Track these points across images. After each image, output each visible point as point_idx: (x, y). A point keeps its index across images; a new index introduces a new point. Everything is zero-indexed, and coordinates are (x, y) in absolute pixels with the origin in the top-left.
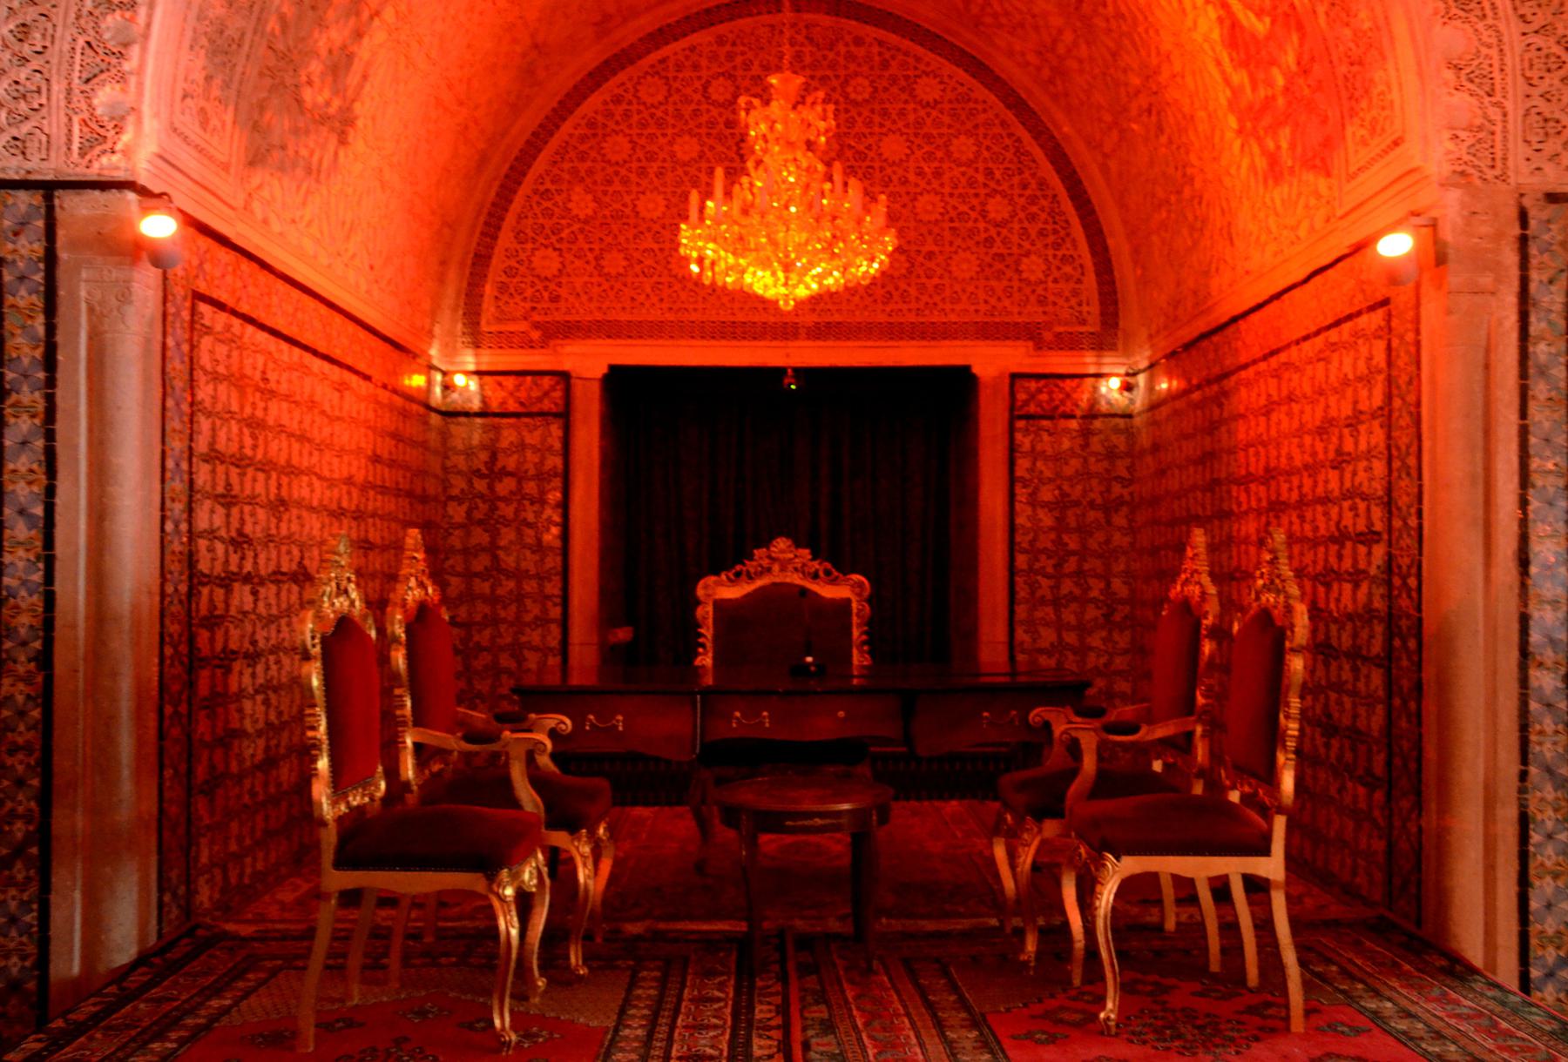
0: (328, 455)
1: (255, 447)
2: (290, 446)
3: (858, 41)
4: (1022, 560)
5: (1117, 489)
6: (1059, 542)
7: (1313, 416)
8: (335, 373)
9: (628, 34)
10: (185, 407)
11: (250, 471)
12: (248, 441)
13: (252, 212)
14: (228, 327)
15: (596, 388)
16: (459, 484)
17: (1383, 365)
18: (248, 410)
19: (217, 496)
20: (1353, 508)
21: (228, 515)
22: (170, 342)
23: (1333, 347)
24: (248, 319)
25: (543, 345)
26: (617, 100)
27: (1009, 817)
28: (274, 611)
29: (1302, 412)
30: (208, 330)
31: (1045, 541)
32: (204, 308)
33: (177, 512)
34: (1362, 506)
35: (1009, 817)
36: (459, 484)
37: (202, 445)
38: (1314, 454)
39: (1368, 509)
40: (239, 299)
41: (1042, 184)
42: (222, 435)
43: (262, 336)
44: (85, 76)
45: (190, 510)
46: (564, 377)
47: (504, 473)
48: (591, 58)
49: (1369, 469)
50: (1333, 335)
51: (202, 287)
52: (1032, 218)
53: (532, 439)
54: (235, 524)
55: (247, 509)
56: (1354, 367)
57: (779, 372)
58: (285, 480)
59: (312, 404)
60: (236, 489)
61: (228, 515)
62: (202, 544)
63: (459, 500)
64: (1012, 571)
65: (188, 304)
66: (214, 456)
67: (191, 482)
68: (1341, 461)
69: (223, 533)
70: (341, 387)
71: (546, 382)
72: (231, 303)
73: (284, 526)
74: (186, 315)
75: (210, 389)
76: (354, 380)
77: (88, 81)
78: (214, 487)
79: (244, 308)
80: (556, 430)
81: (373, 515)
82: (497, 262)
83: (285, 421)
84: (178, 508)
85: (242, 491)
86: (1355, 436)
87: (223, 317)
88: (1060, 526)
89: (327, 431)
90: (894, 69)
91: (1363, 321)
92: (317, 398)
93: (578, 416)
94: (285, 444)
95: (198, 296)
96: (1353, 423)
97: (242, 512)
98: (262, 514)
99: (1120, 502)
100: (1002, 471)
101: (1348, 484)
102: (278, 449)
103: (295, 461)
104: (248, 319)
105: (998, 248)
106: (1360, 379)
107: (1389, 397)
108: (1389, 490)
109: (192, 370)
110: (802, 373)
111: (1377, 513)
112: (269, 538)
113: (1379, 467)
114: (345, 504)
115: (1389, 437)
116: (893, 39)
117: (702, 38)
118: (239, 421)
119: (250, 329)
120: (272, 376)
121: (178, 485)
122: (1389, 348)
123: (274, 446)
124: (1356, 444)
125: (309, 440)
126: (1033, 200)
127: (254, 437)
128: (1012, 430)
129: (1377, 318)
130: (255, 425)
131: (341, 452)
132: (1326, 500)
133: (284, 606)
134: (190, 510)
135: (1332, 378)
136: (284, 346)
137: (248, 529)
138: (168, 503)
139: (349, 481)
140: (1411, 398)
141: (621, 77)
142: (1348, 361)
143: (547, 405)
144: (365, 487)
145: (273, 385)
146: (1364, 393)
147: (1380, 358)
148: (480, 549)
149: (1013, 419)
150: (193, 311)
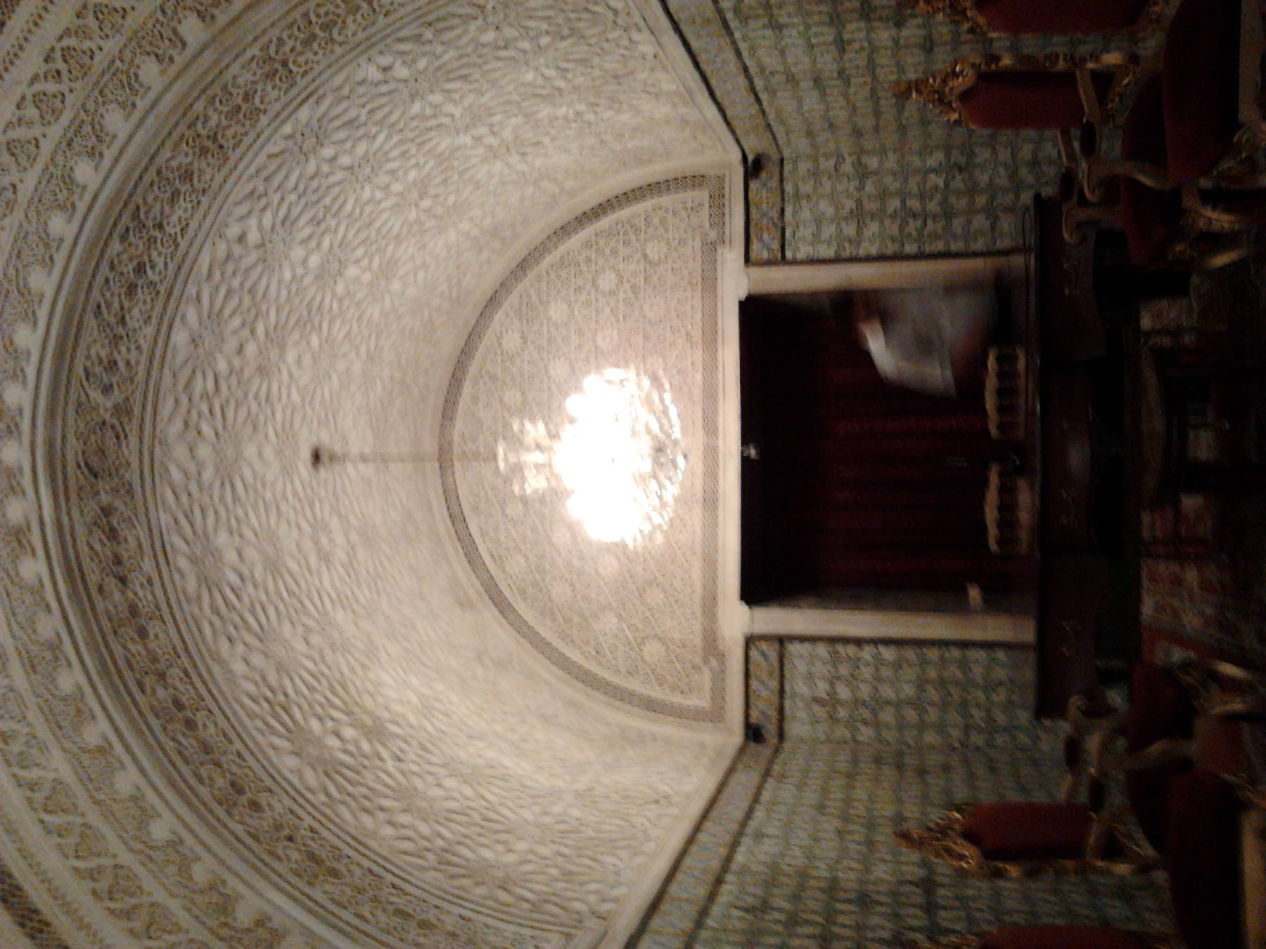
4: (910, 248)
5: (847, 167)
8: (746, 841)
13: (608, 912)
16: (841, 732)
24: (699, 924)
25: (721, 657)
27: (1178, 248)
28: (963, 914)
31: (894, 229)
35: (1178, 248)
36: (841, 732)
52: (615, 252)
53: (801, 666)
57: (746, 462)
58: (842, 895)
63: (854, 730)
64: (920, 256)
70: (759, 836)
71: (754, 654)
73: (882, 899)
88: (878, 215)
99: (858, 164)
110: (746, 438)
112: (896, 916)
119: (710, 922)
123: (812, 904)
128: (795, 262)
130: (793, 921)
133: (956, 903)
136: (725, 888)
139: (840, 833)
149: (784, 261)
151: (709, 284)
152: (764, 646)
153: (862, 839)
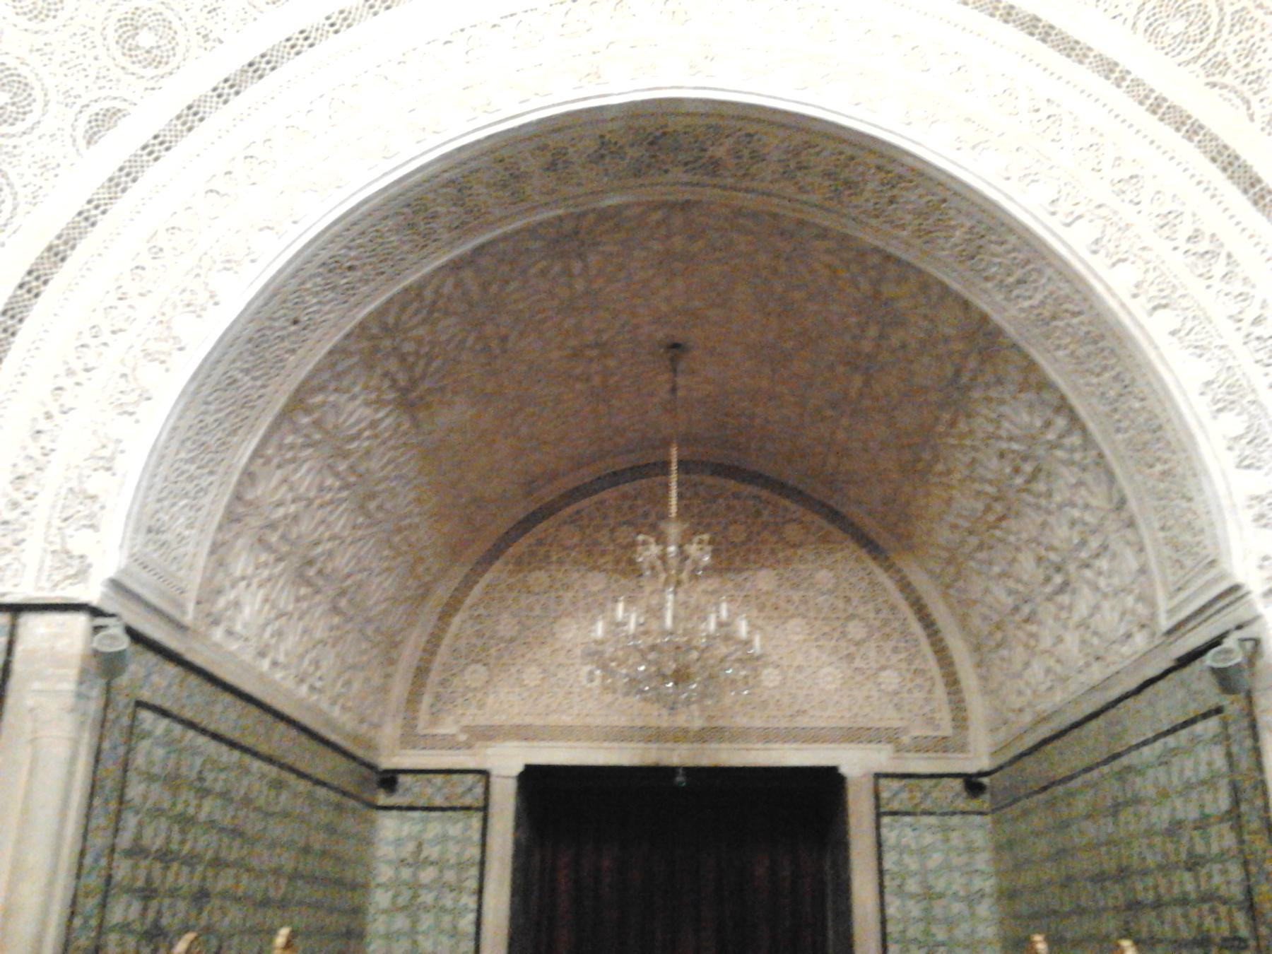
0: (259, 848)
1: (183, 842)
2: (220, 840)
3: (736, 496)
6: (926, 932)
7: (1161, 817)
8: (273, 771)
9: (549, 493)
10: (113, 805)
11: (175, 866)
12: (176, 837)
14: (168, 732)
15: (512, 786)
17: (1225, 769)
18: (180, 808)
19: (135, 891)
20: (1213, 911)
21: (145, 909)
22: (106, 745)
23: (1174, 752)
24: (190, 725)
25: (468, 746)
26: (540, 542)
29: (1149, 814)
30: (146, 735)
31: (913, 932)
32: (147, 716)
33: (88, 908)
34: (1223, 910)
37: (125, 840)
38: (1166, 855)
39: (1230, 913)
40: (183, 707)
41: (893, 608)
42: (148, 833)
43: (202, 740)
44: (64, 516)
45: (103, 905)
46: (484, 774)
47: (429, 862)
48: (520, 512)
49: (1224, 872)
50: (1171, 741)
51: (146, 695)
53: (455, 830)
54: (151, 915)
55: (167, 901)
56: (1196, 770)
57: (670, 771)
59: (247, 801)
60: (157, 884)
61: (145, 909)
62: (113, 938)
65: (130, 710)
66: (137, 851)
67: (109, 878)
68: (1194, 864)
69: (137, 927)
70: (278, 785)
71: (470, 779)
72: (175, 709)
74: (125, 721)
75: (142, 787)
76: (291, 778)
77: (66, 520)
78: (134, 879)
79: (188, 714)
80: (475, 821)
81: (300, 903)
82: (434, 677)
83: (217, 816)
84: (90, 904)
85: (163, 882)
86: (1207, 840)
87: (164, 723)
88: (928, 918)
89: (259, 826)
90: (766, 515)
91: (1199, 728)
92: (253, 795)
93: (494, 810)
94: (215, 838)
95: (140, 704)
96: (1202, 824)
97: (161, 905)
98: (182, 906)
100: (873, 864)
101: (1204, 886)
102: (204, 842)
103: (223, 855)
104: (190, 725)
105: (858, 663)
106: (1203, 783)
107: (1236, 802)
108: (1249, 891)
109: (125, 771)
110: (694, 773)
111: (1241, 919)
113: (1236, 872)
114: (272, 893)
115: (1241, 842)
116: (765, 494)
117: (609, 495)
118: (169, 818)
119: (191, 734)
120: (210, 776)
121: (93, 881)
122: (1229, 755)
123: (202, 842)
124: (1208, 844)
125: (242, 834)
126: (886, 622)
127: (183, 832)
128: (878, 827)
129: (1213, 724)
131: (273, 845)
132: (1184, 901)
134: (103, 905)
135: (1175, 781)
136: (224, 749)
137: (165, 922)
138: (81, 900)
139: (277, 872)
140: (1259, 802)
141: (544, 525)
142: (1189, 764)
143: (468, 801)
144: (294, 876)
145: (207, 784)
146: (1208, 797)
147: (1220, 762)
148: (399, 934)
149: (879, 815)
150: (134, 717)
151: (854, 735)
152: (479, 790)
153: (185, 869)
